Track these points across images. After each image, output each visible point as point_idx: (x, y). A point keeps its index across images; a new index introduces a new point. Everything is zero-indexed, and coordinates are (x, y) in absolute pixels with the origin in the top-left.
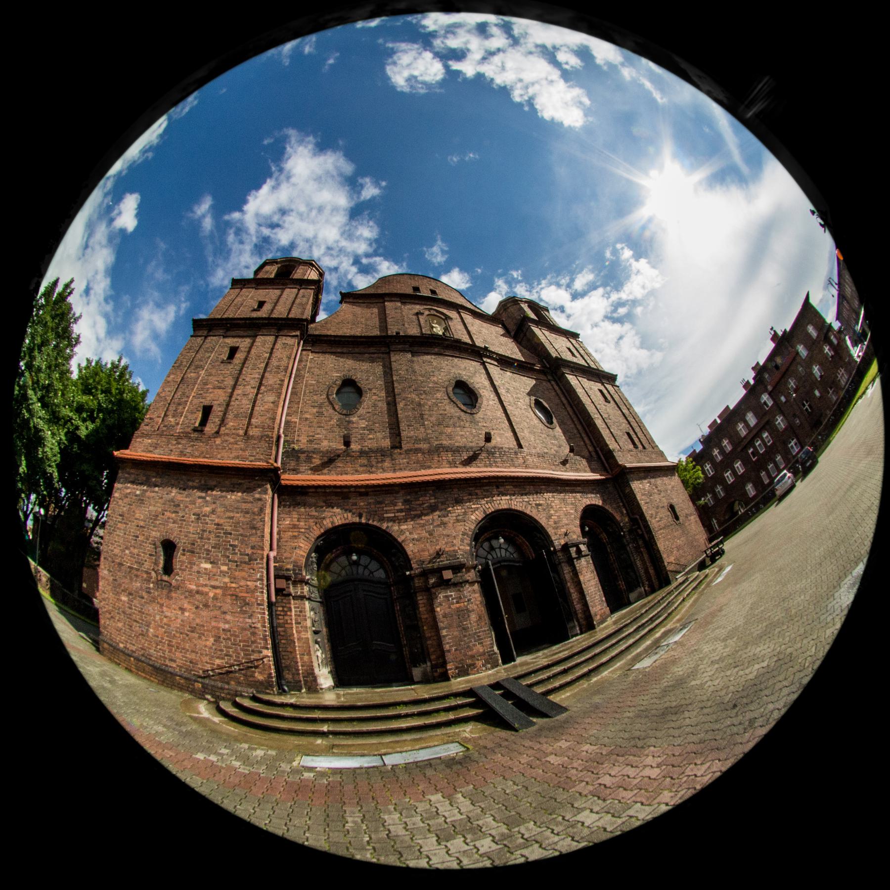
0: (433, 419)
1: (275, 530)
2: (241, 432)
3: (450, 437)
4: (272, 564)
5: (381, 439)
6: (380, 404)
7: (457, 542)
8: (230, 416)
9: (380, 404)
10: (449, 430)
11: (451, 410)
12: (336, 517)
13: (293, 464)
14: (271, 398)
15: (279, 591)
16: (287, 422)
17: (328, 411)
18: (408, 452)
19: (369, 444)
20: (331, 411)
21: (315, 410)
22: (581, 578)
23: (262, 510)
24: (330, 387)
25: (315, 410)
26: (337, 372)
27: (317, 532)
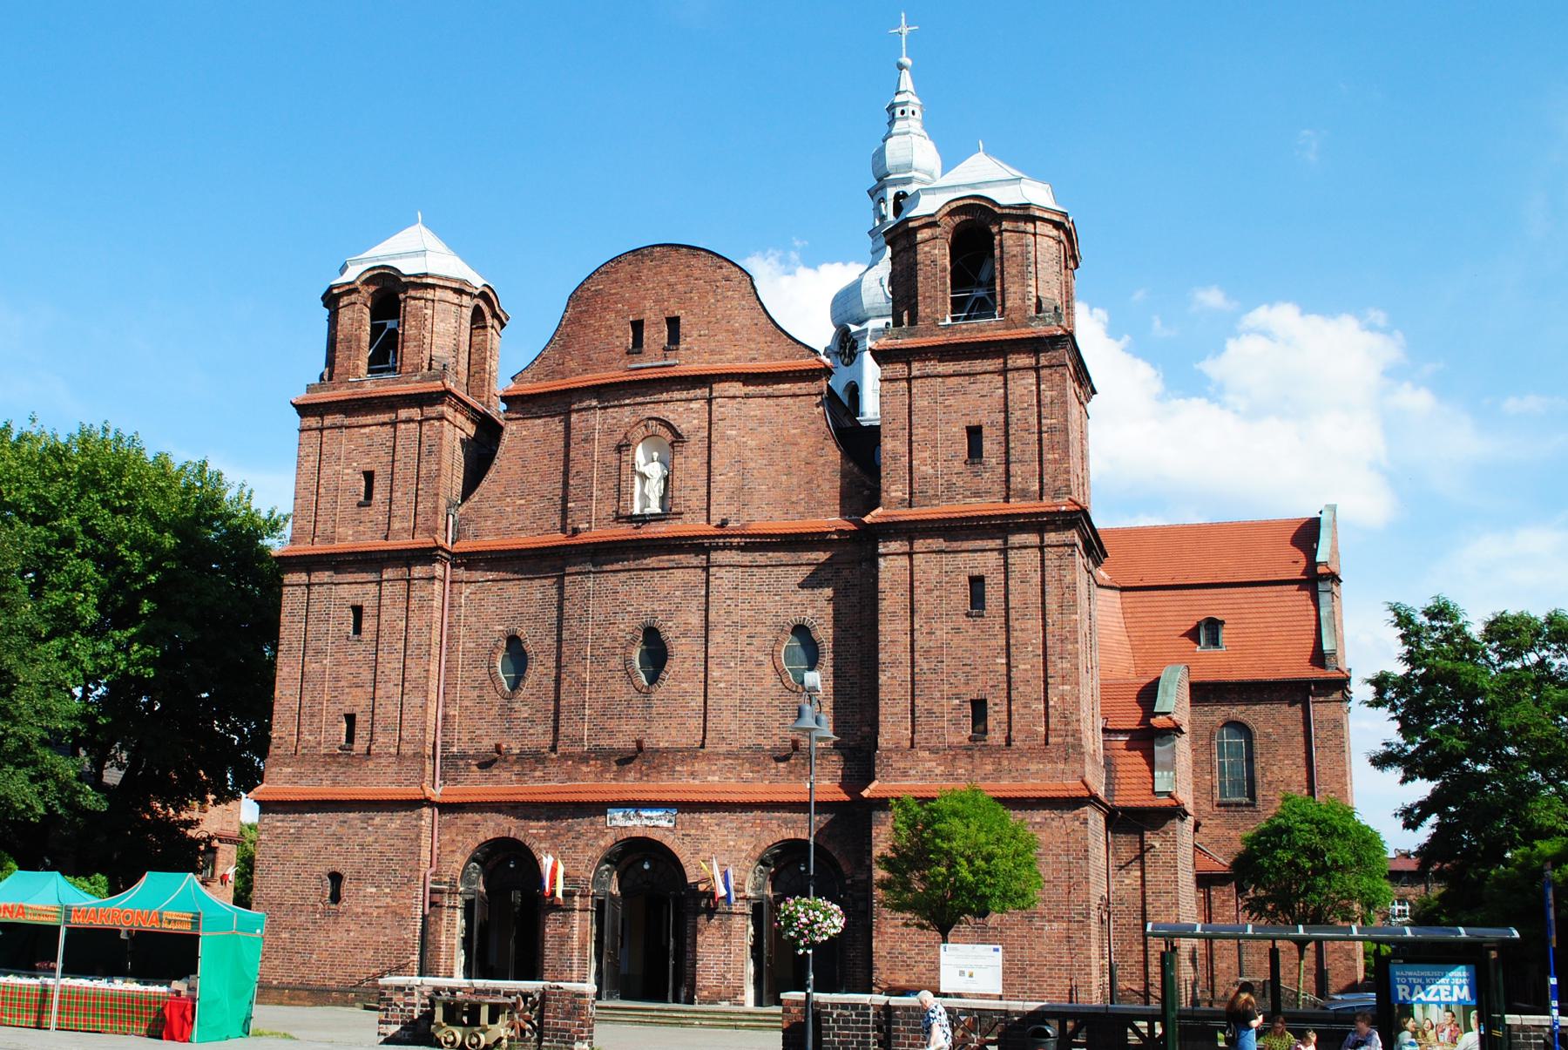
0: (598, 706)
1: (436, 845)
2: (393, 750)
3: (611, 734)
4: (429, 886)
5: (540, 737)
6: (545, 680)
7: (582, 868)
8: (378, 729)
9: (545, 680)
10: (613, 724)
11: (621, 689)
12: (493, 827)
13: (452, 772)
14: (419, 701)
15: (432, 904)
16: (445, 717)
17: (490, 695)
18: (566, 756)
19: (530, 743)
20: (493, 693)
21: (476, 693)
22: (699, 939)
23: (418, 837)
24: (492, 652)
25: (476, 693)
26: (501, 620)
27: (472, 844)
